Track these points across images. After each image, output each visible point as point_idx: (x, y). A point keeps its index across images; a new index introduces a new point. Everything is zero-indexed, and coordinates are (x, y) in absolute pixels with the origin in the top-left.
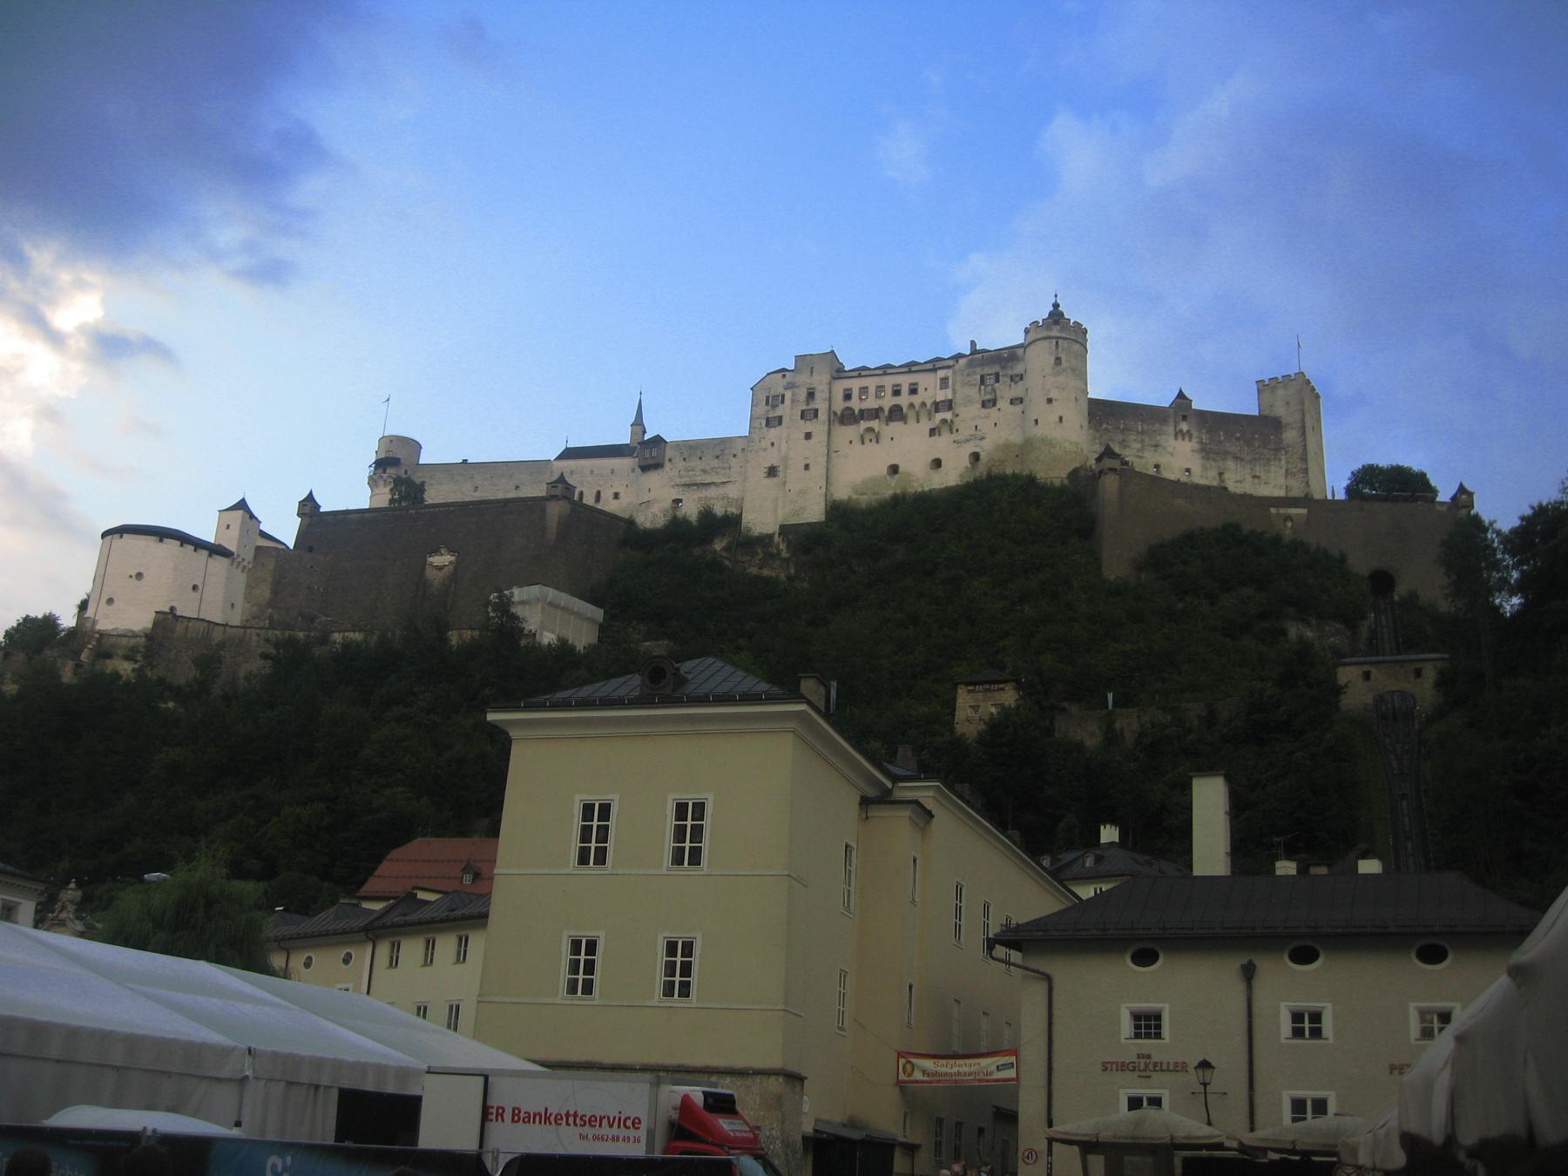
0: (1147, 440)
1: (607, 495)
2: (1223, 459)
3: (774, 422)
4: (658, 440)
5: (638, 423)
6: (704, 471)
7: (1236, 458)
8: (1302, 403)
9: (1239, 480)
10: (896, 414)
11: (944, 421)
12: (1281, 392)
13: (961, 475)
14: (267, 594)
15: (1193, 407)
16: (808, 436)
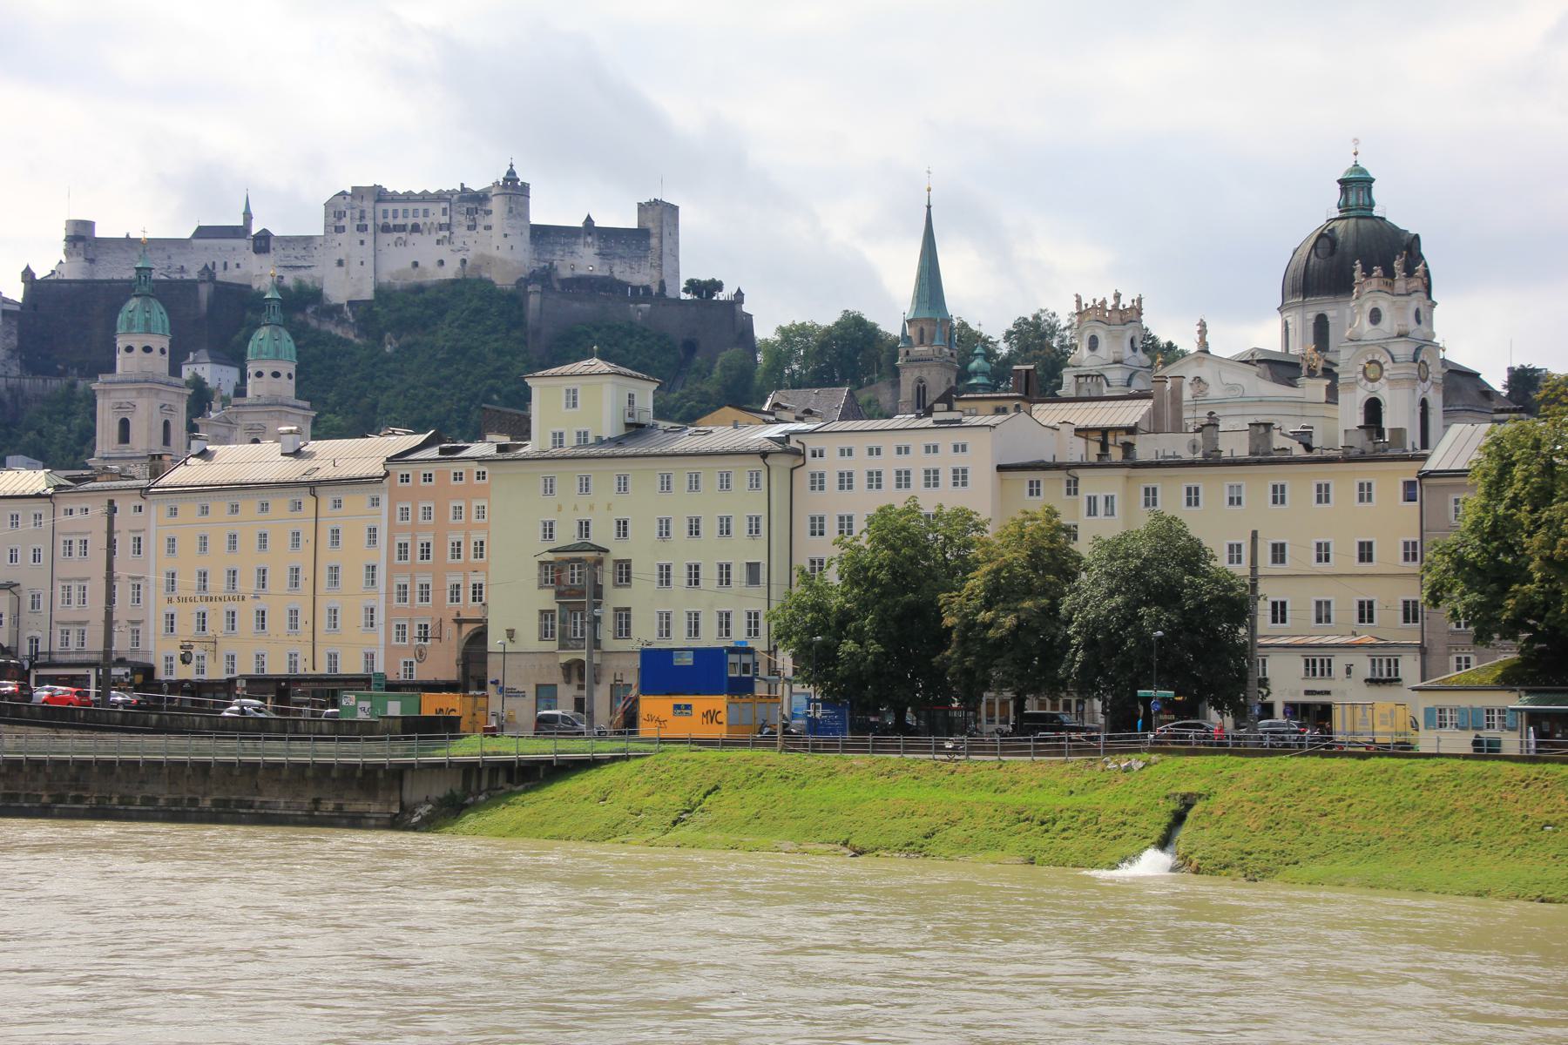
0: (567, 250)
1: (232, 265)
2: (614, 258)
3: (340, 229)
4: (265, 236)
5: (248, 216)
6: (296, 257)
7: (621, 257)
8: (662, 222)
9: (621, 272)
10: (416, 228)
11: (445, 237)
12: (650, 212)
13: (456, 273)
14: (16, 343)
15: (596, 225)
16: (362, 243)
